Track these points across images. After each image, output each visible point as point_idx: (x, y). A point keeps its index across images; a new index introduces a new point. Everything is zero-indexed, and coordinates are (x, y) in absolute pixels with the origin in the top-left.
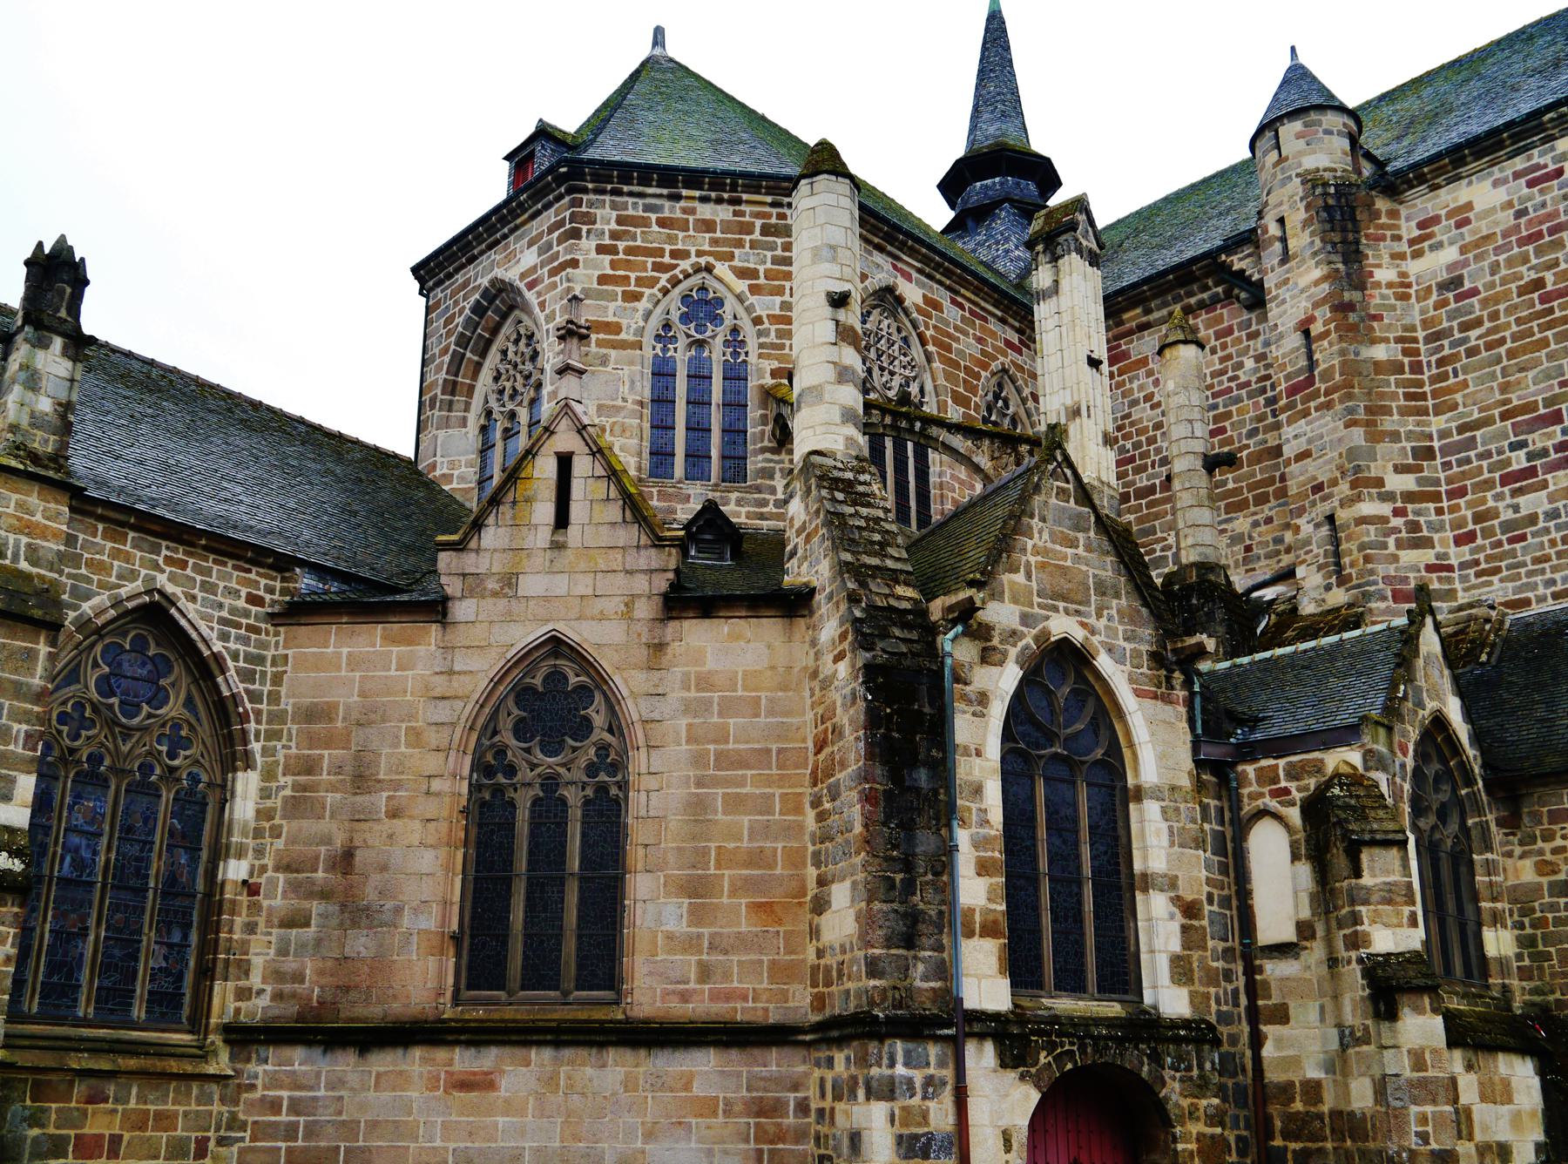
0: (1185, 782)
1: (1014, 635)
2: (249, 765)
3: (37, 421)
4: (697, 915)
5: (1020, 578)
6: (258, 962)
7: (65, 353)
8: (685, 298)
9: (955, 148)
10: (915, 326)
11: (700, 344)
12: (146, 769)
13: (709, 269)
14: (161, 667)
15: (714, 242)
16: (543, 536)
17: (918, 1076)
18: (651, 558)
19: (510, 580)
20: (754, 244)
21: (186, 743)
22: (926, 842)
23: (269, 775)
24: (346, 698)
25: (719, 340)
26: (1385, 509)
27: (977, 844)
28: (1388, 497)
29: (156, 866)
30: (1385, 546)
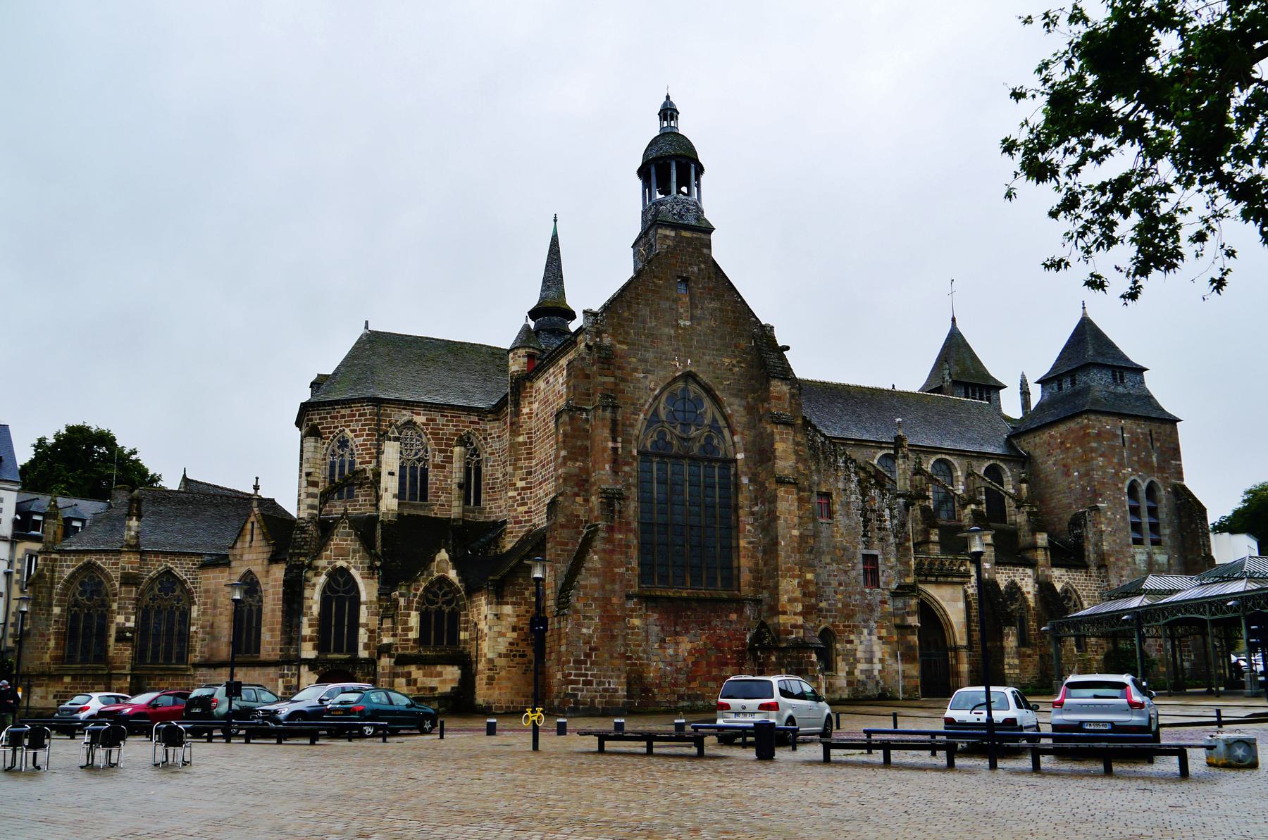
0: (375, 599)
1: (325, 568)
2: (194, 603)
3: (132, 537)
4: (272, 636)
5: (328, 553)
6: (197, 649)
7: (137, 520)
8: (339, 441)
9: (533, 301)
10: (422, 430)
11: (342, 456)
12: (172, 607)
13: (344, 430)
14: (174, 583)
15: (345, 422)
16: (247, 545)
17: (290, 673)
18: (266, 549)
19: (242, 556)
20: (356, 421)
21: (182, 600)
22: (295, 621)
23: (199, 606)
24: (212, 587)
25: (347, 454)
26: (515, 494)
27: (309, 620)
28: (516, 489)
29: (176, 628)
30: (513, 506)
